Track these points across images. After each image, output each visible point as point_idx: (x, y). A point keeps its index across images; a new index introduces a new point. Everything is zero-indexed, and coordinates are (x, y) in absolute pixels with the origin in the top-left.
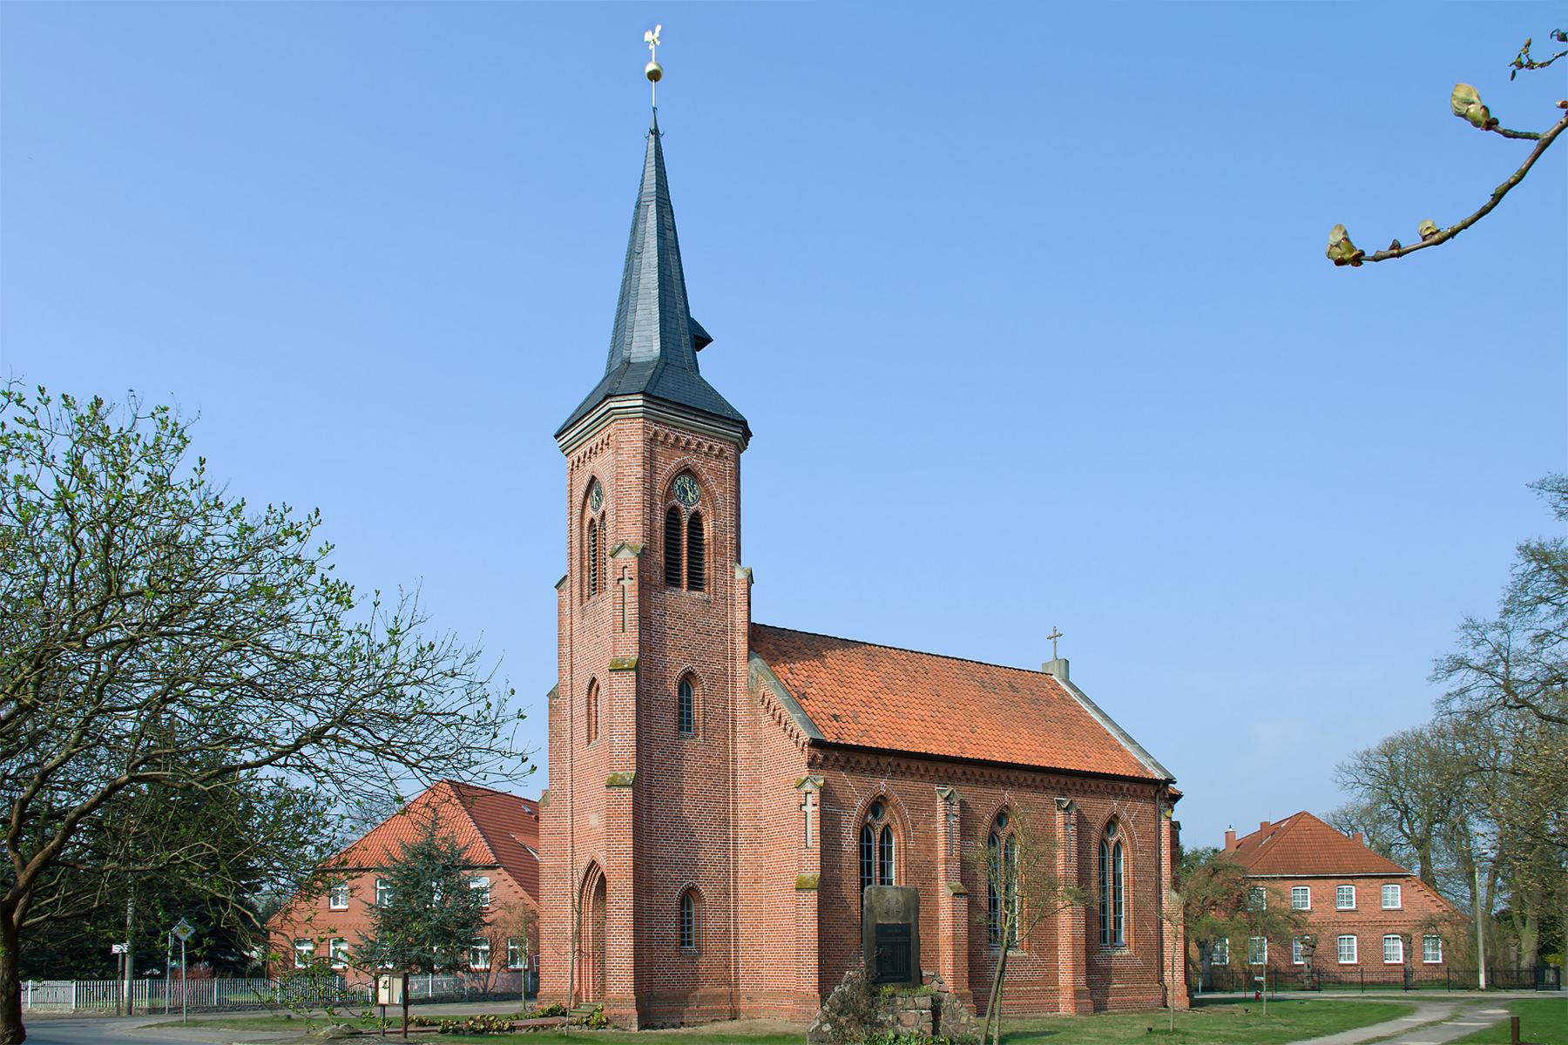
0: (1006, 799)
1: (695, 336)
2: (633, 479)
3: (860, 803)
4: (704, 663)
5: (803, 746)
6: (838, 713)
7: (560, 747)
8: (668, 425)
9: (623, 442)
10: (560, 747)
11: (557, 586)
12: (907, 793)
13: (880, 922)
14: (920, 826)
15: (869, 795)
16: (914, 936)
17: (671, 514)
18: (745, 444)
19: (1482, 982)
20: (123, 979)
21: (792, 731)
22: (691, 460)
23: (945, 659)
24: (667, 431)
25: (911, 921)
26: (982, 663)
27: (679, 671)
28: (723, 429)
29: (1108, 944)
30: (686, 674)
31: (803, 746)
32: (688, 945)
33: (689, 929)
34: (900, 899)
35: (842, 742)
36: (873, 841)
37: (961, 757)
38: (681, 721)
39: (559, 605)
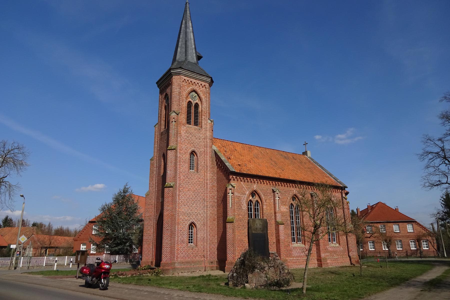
0: (295, 192)
1: (198, 56)
2: (177, 92)
3: (247, 193)
4: (198, 148)
5: (229, 173)
6: (240, 164)
7: (153, 176)
8: (189, 77)
9: (174, 82)
10: (153, 176)
11: (155, 126)
12: (263, 190)
13: (254, 232)
14: (268, 201)
15: (251, 190)
16: (266, 237)
17: (189, 103)
18: (212, 85)
19: (446, 256)
20: (13, 256)
21: (225, 169)
22: (196, 88)
23: (273, 150)
24: (188, 79)
25: (265, 232)
26: (284, 152)
27: (190, 151)
28: (204, 78)
29: (331, 242)
30: (192, 151)
31: (229, 173)
32: (191, 243)
33: (192, 237)
34: (261, 224)
35: (241, 172)
36: (252, 206)
37: (279, 178)
38: (191, 167)
39: (155, 132)
